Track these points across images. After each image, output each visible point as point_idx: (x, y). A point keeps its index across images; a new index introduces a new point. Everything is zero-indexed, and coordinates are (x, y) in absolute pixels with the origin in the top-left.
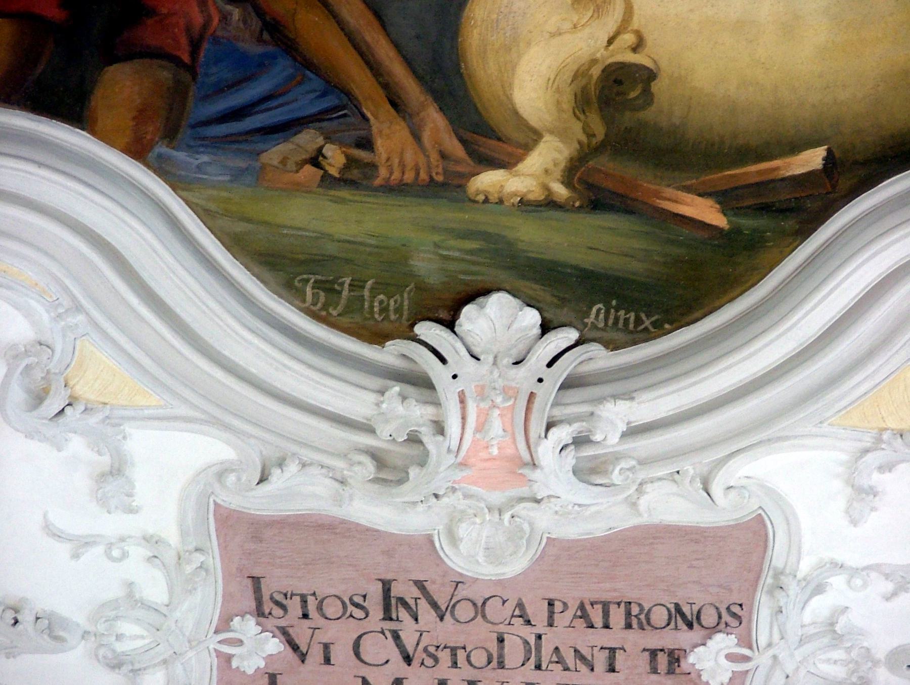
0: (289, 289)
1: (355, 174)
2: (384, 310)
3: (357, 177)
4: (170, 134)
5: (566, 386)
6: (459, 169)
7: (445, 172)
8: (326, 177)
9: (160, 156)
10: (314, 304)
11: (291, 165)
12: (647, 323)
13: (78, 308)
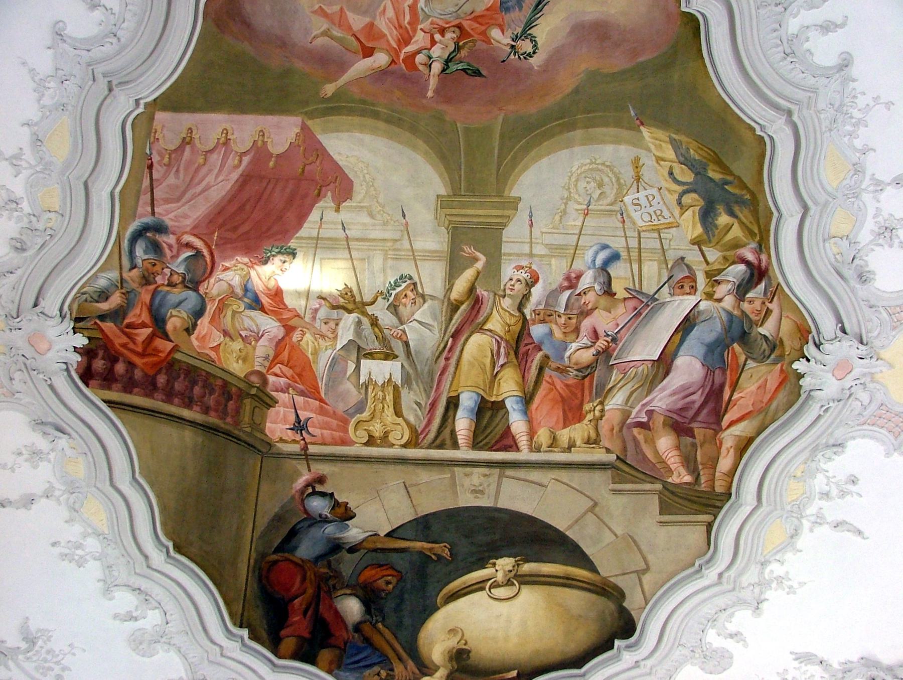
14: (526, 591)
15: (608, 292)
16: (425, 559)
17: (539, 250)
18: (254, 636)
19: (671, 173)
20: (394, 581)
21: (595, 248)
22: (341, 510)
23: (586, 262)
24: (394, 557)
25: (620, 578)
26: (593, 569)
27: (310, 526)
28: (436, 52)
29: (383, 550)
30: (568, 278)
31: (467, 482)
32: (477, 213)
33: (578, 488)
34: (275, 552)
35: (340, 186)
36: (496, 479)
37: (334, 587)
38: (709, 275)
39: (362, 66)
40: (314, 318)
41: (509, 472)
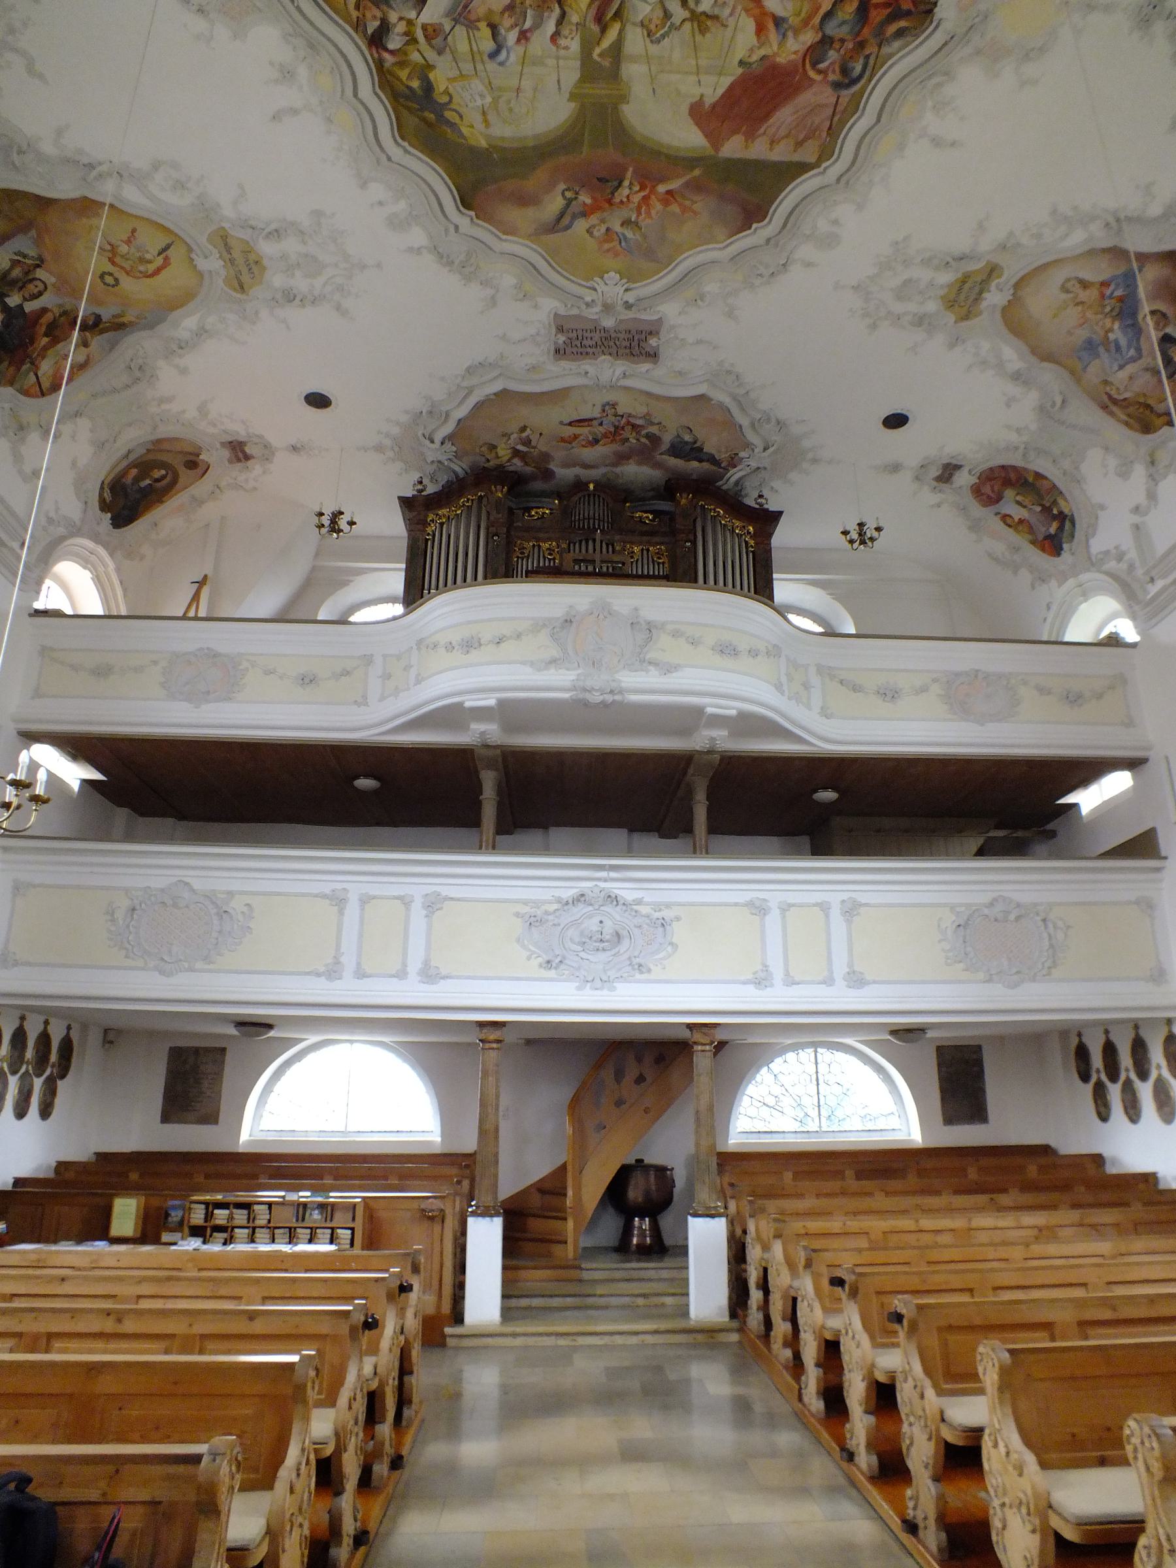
15: (493, 27)
17: (551, 62)
19: (461, 117)
21: (508, 64)
23: (513, 53)
28: (626, 192)
30: (527, 39)
32: (600, 90)
35: (698, 112)
38: (414, 41)
39: (674, 185)
40: (734, 8)
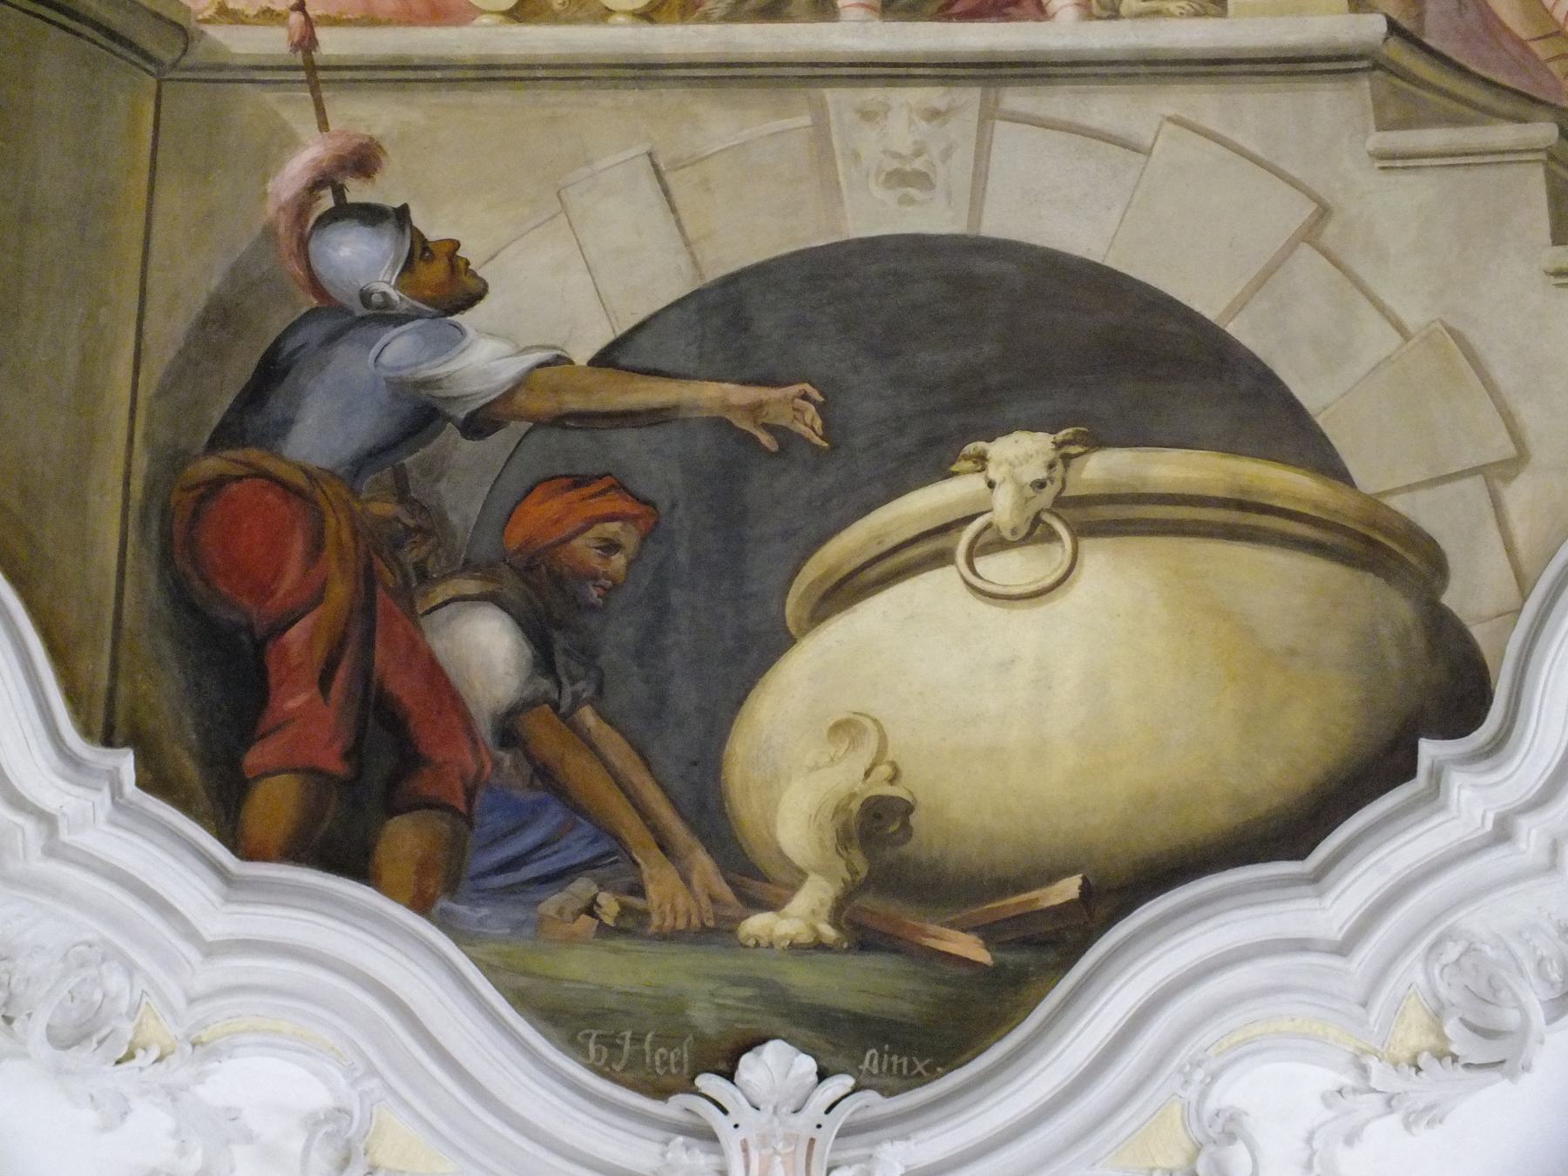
0: (573, 1045)
1: (629, 923)
2: (665, 1063)
3: (632, 925)
4: (452, 887)
5: (841, 1134)
6: (729, 913)
7: (715, 915)
8: (602, 926)
9: (443, 910)
10: (598, 1059)
11: (568, 915)
12: (920, 1067)
13: (372, 1071)
14: (1099, 557)
16: (733, 451)
18: (156, 780)
20: (629, 537)
22: (434, 273)
24: (627, 440)
25: (1423, 496)
26: (1330, 466)
27: (332, 339)
29: (586, 420)
31: (869, 142)
33: (1256, 150)
34: (214, 445)
36: (973, 126)
37: (423, 575)
41: (1016, 99)
